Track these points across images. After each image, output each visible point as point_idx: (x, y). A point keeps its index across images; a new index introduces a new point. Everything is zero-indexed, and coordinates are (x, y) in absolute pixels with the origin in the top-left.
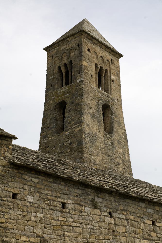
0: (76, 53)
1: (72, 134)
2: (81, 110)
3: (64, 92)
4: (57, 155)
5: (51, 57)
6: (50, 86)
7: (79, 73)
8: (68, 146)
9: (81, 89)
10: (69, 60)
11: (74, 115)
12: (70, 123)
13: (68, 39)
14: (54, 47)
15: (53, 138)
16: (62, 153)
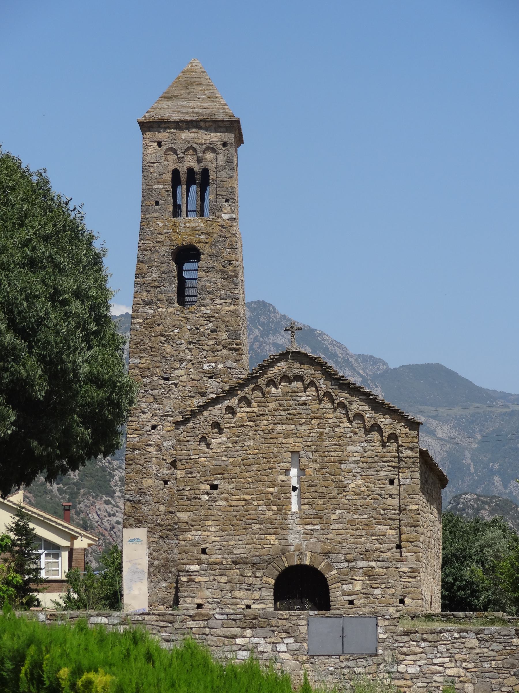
0: (221, 159)
1: (216, 315)
2: (236, 276)
3: (194, 228)
4: (183, 346)
5: (156, 144)
6: (154, 203)
7: (227, 201)
8: (208, 335)
9: (234, 235)
10: (202, 165)
11: (220, 280)
12: (209, 293)
13: (202, 124)
14: (164, 125)
15: (170, 310)
16: (195, 343)
